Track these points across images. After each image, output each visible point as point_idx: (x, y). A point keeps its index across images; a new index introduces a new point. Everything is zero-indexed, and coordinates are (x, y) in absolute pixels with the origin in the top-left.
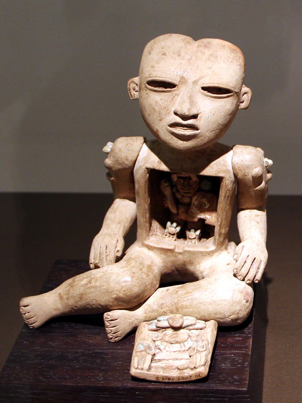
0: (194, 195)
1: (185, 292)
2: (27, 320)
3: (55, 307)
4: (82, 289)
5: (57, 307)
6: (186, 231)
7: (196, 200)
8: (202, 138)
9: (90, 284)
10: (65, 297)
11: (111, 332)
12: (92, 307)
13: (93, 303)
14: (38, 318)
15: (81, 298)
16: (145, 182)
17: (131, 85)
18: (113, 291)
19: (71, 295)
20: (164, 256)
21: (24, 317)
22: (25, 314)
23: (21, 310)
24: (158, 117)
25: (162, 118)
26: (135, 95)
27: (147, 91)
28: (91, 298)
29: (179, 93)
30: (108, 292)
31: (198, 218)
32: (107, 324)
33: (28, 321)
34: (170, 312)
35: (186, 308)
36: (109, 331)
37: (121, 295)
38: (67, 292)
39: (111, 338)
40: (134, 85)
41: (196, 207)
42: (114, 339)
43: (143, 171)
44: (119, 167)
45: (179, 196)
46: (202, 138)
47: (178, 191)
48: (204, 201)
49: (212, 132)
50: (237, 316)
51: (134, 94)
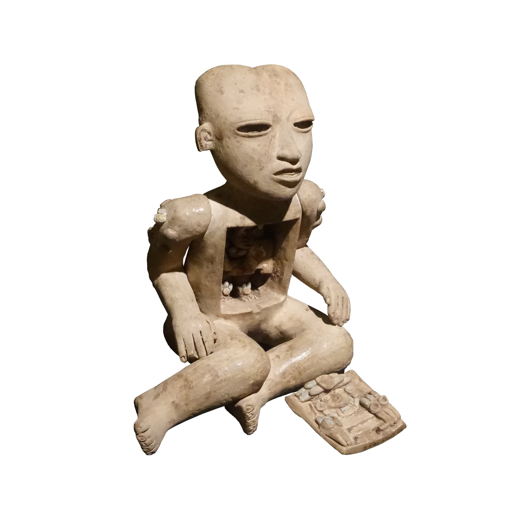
3: (169, 420)
6: (239, 288)
9: (218, 378)
10: (182, 403)
15: (207, 398)
17: (201, 134)
18: (250, 377)
19: (191, 399)
20: (241, 322)
24: (258, 166)
26: (207, 145)
27: (238, 139)
28: (223, 394)
31: (256, 270)
34: (293, 379)
35: (309, 369)
40: (205, 133)
44: (187, 236)
48: (262, 249)
51: (206, 145)
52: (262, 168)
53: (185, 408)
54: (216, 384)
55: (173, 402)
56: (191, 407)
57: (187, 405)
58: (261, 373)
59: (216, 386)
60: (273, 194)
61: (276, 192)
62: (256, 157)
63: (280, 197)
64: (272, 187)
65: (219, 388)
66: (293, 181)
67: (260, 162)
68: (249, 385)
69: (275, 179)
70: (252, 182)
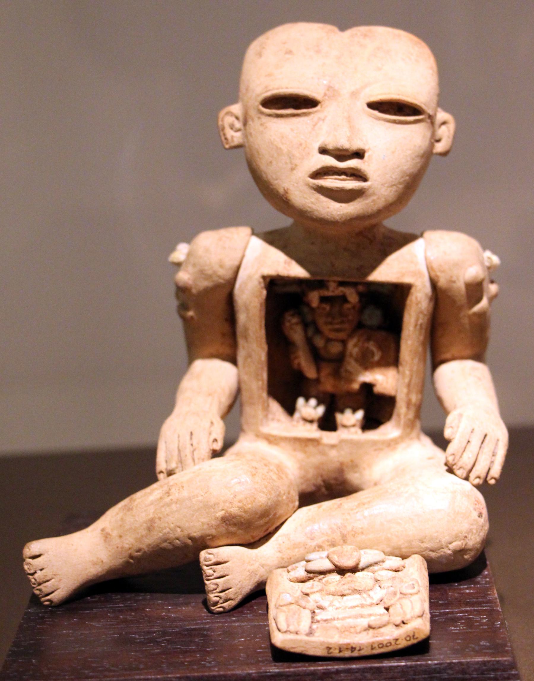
0: (350, 336)
1: (356, 504)
2: (39, 587)
3: (95, 559)
4: (152, 509)
5: (98, 558)
7: (355, 345)
8: (375, 198)
9: (168, 496)
10: (115, 533)
11: (216, 589)
12: (173, 545)
13: (177, 536)
14: (60, 580)
15: (150, 529)
16: (261, 304)
18: (218, 504)
19: (127, 527)
21: (33, 580)
22: (32, 574)
23: (26, 567)
24: (286, 163)
25: (296, 165)
28: (172, 525)
29: (326, 117)
30: (207, 506)
32: (208, 571)
33: (40, 590)
34: (330, 545)
35: (362, 533)
36: (212, 587)
37: (234, 510)
38: (120, 523)
39: (216, 604)
41: (356, 360)
42: (221, 603)
43: (256, 283)
45: (319, 342)
46: (375, 198)
47: (318, 331)
49: (391, 188)
50: (464, 544)
52: (294, 166)
53: (116, 541)
54: (163, 506)
55: (103, 530)
56: (127, 542)
57: (121, 537)
58: (239, 502)
59: (163, 509)
60: (310, 212)
61: (314, 207)
62: (284, 148)
63: (322, 216)
64: (308, 199)
65: (167, 515)
66: (337, 188)
67: (291, 156)
68: (217, 518)
69: (311, 185)
70: (281, 191)
